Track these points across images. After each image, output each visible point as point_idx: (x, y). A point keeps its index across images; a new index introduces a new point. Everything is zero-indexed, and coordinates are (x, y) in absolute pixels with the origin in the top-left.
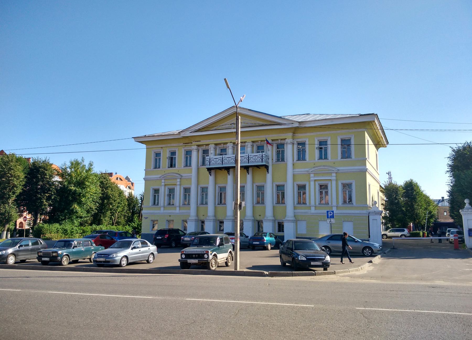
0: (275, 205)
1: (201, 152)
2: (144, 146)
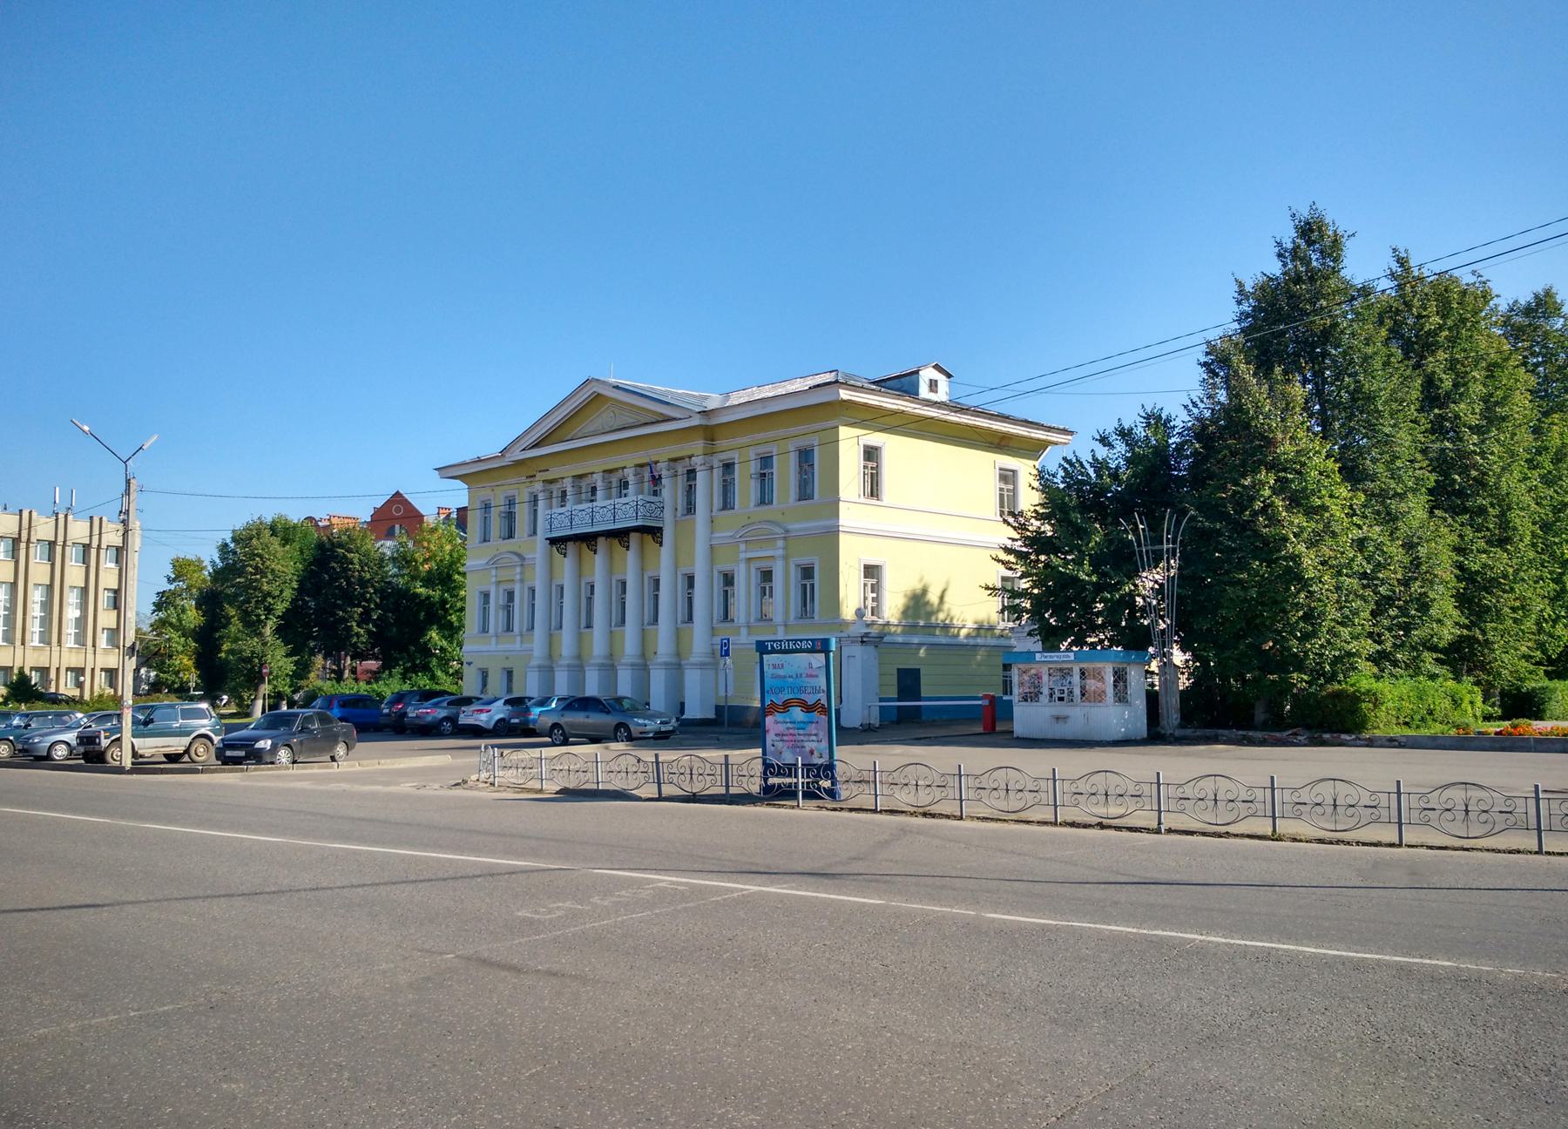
0: (680, 625)
1: (717, 473)
2: (458, 484)
